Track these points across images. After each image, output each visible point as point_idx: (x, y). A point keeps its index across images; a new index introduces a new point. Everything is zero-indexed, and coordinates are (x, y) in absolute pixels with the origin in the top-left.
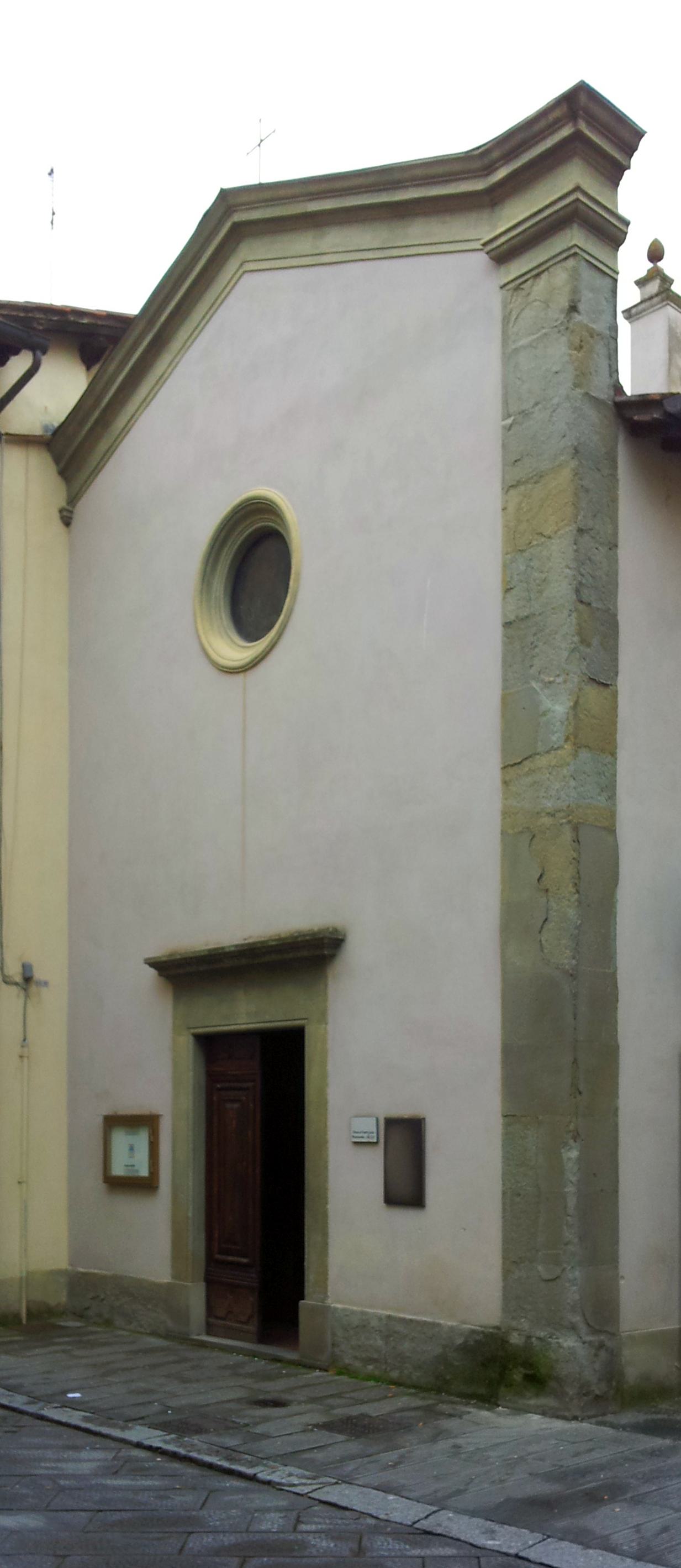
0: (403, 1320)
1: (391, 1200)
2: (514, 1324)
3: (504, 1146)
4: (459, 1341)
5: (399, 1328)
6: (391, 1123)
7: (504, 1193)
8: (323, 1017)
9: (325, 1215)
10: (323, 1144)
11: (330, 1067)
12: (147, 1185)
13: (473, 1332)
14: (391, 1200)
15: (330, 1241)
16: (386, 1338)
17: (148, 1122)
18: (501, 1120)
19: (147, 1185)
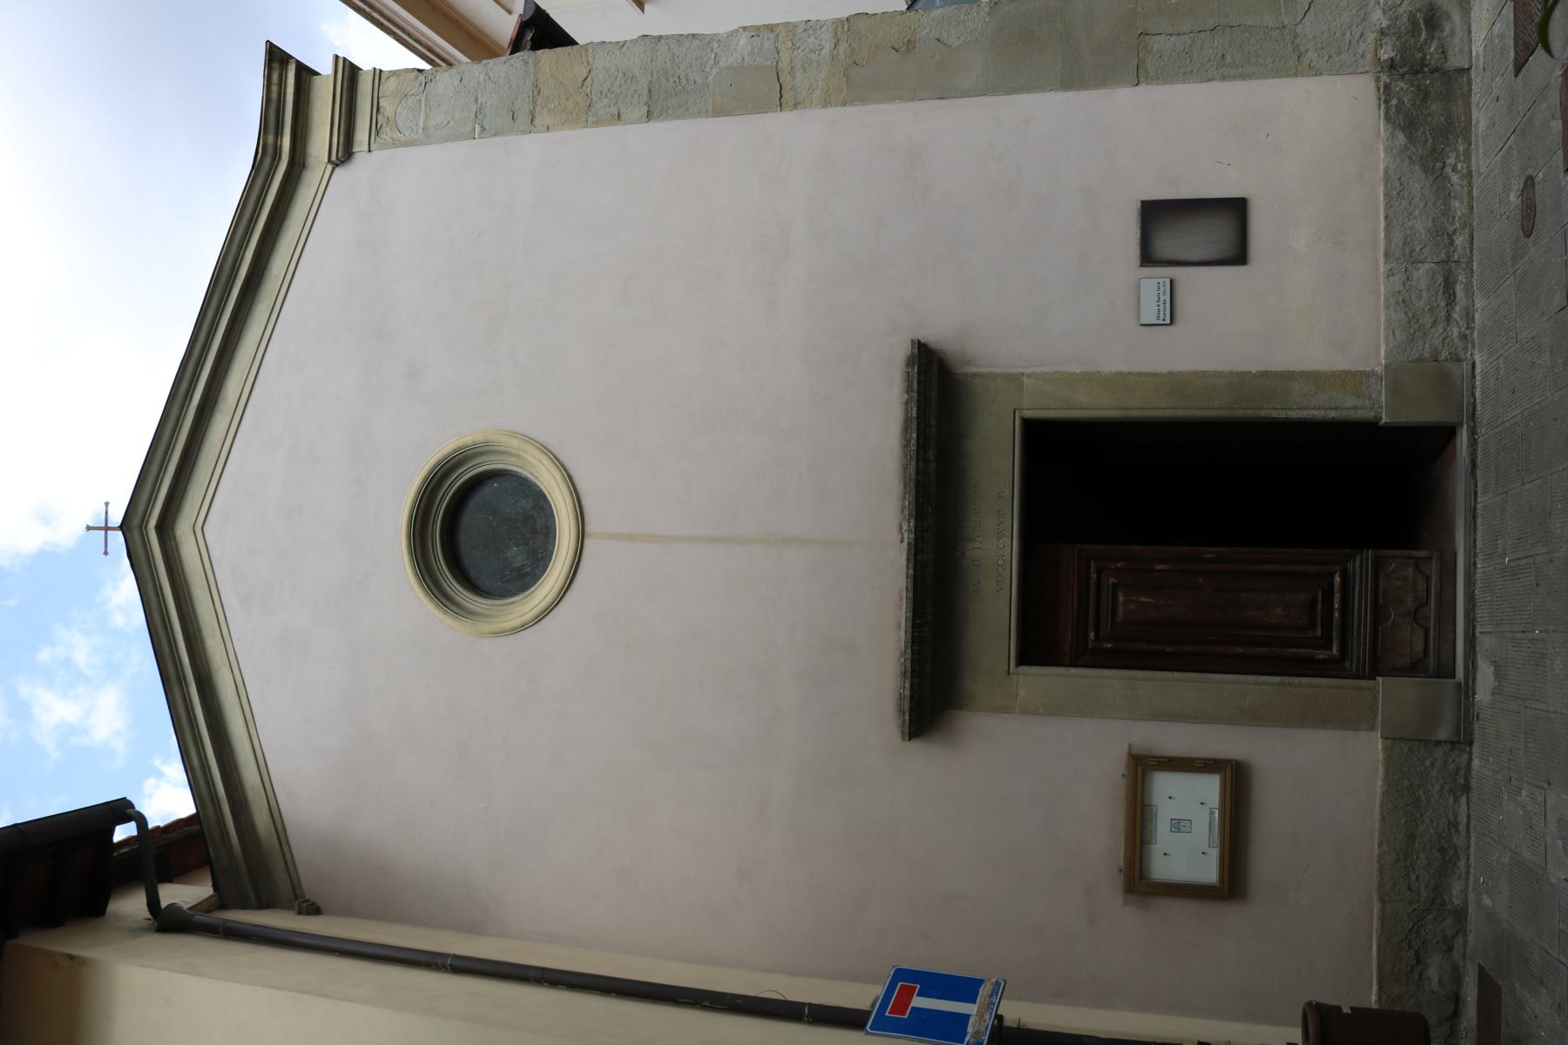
0: (1388, 238)
1: (1239, 257)
2: (1370, 56)
3: (1172, 82)
4: (1401, 138)
5: (1398, 239)
6: (1148, 258)
7: (1223, 78)
8: (1014, 380)
9: (1265, 375)
10: (1175, 382)
11: (1076, 368)
12: (1237, 782)
13: (1388, 119)
14: (1239, 257)
15: (1299, 368)
16: (1412, 260)
17: (1142, 766)
18: (1143, 88)
19: (1237, 782)
